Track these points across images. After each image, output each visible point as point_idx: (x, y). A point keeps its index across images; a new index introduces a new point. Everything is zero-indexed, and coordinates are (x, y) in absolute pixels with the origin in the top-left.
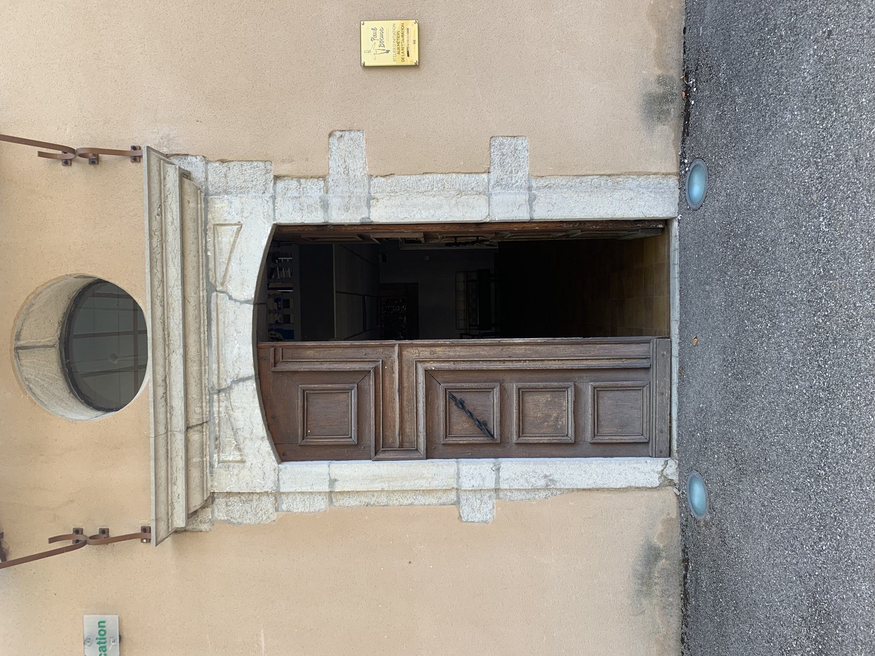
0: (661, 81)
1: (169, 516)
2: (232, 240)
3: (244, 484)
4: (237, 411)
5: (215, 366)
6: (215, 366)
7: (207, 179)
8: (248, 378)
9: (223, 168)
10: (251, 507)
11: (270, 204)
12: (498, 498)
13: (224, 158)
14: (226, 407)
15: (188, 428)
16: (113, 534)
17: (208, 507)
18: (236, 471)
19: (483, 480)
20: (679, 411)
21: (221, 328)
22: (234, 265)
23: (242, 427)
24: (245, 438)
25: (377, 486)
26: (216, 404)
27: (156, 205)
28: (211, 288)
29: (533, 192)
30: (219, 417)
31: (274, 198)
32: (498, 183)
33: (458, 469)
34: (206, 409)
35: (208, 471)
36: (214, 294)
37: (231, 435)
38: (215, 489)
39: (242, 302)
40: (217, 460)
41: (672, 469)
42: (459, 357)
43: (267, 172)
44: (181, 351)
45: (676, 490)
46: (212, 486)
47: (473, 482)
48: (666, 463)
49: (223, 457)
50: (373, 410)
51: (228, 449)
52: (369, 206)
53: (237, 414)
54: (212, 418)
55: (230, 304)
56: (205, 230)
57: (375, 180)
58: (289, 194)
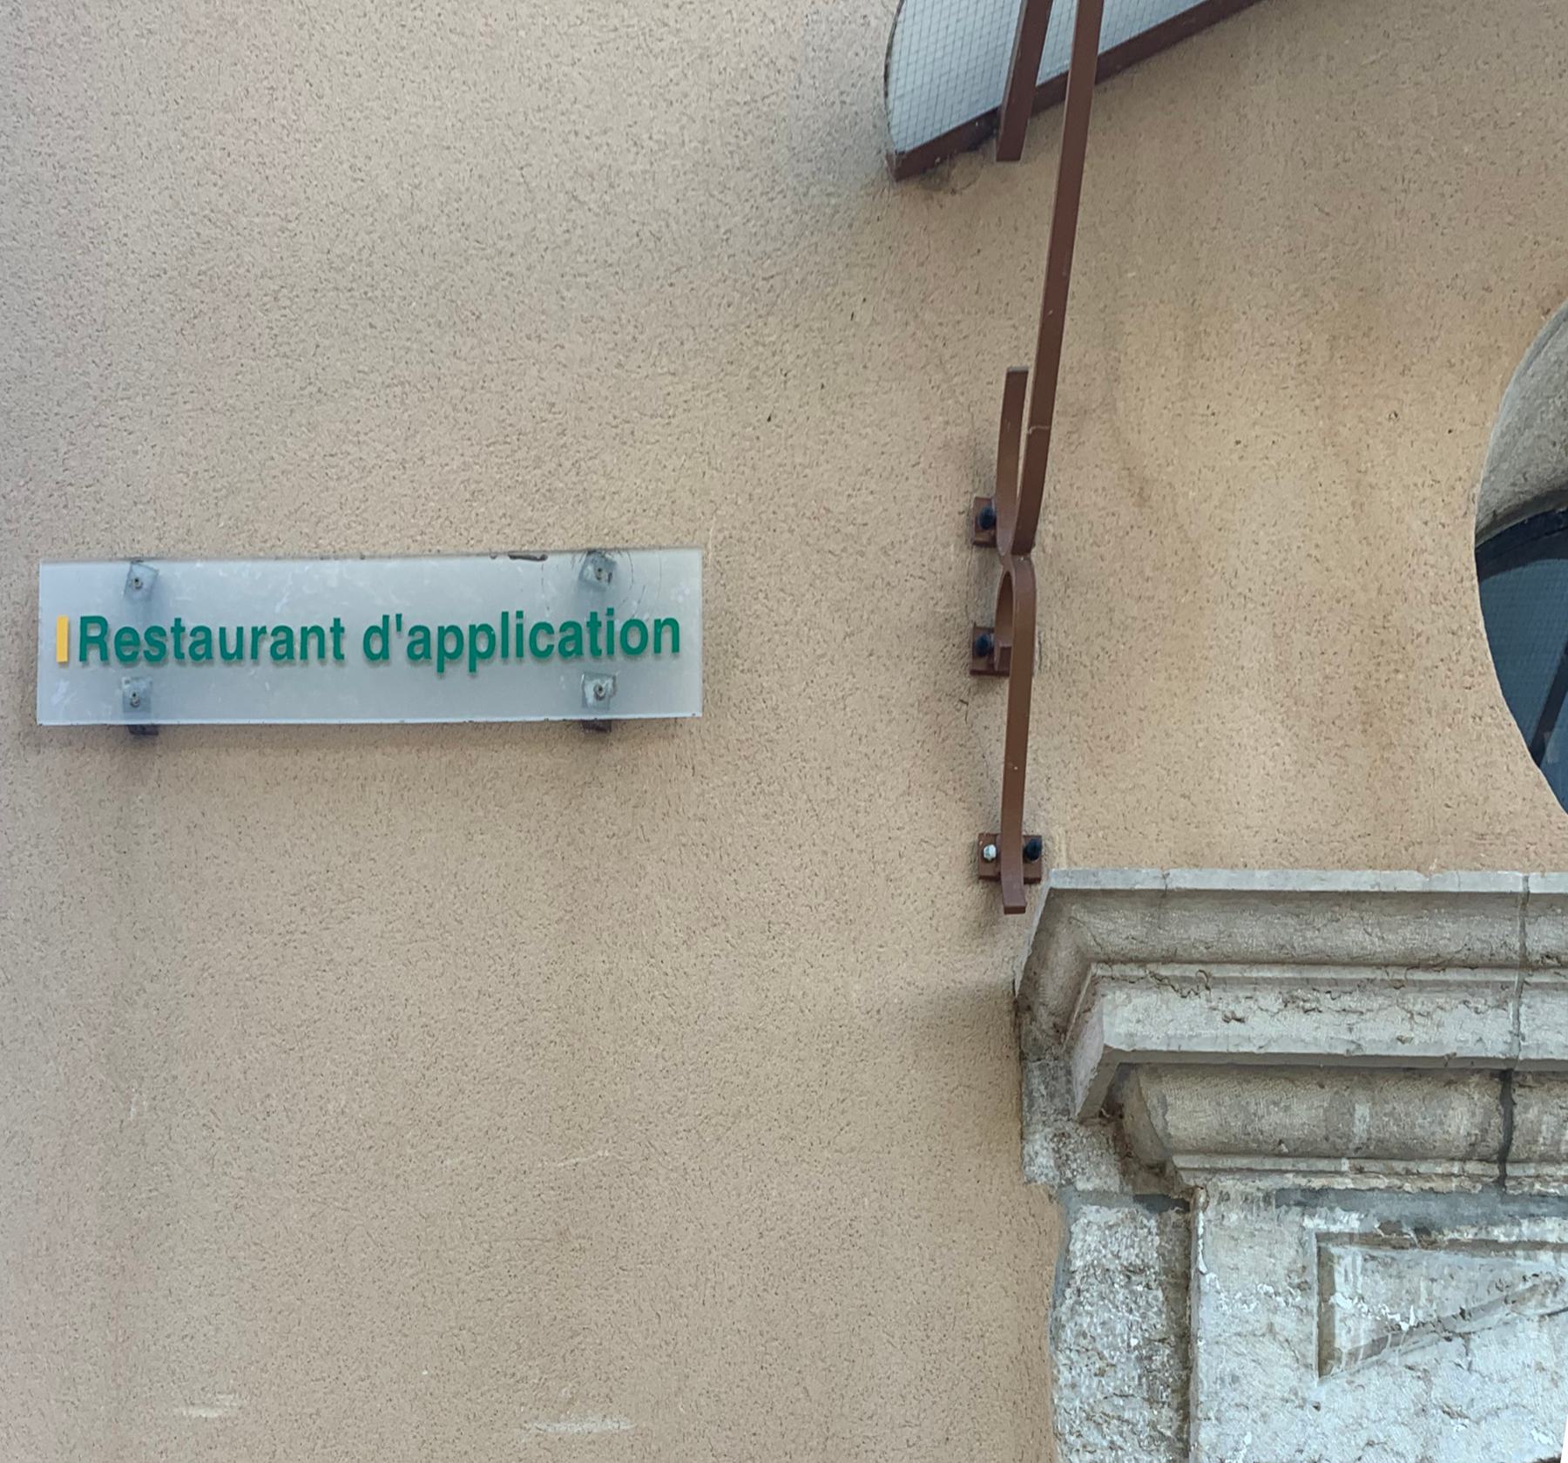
3: (1232, 1365)
4: (1545, 1338)
10: (1124, 1396)
17: (1124, 1173)
18: (1287, 1323)
23: (1478, 1364)
24: (1426, 1376)
30: (1513, 1246)
35: (1290, 1180)
37: (1441, 1305)
38: (1210, 1213)
40: (1334, 1229)
46: (1225, 1197)
49: (1348, 1260)
51: (1383, 1286)
54: (1514, 1208)
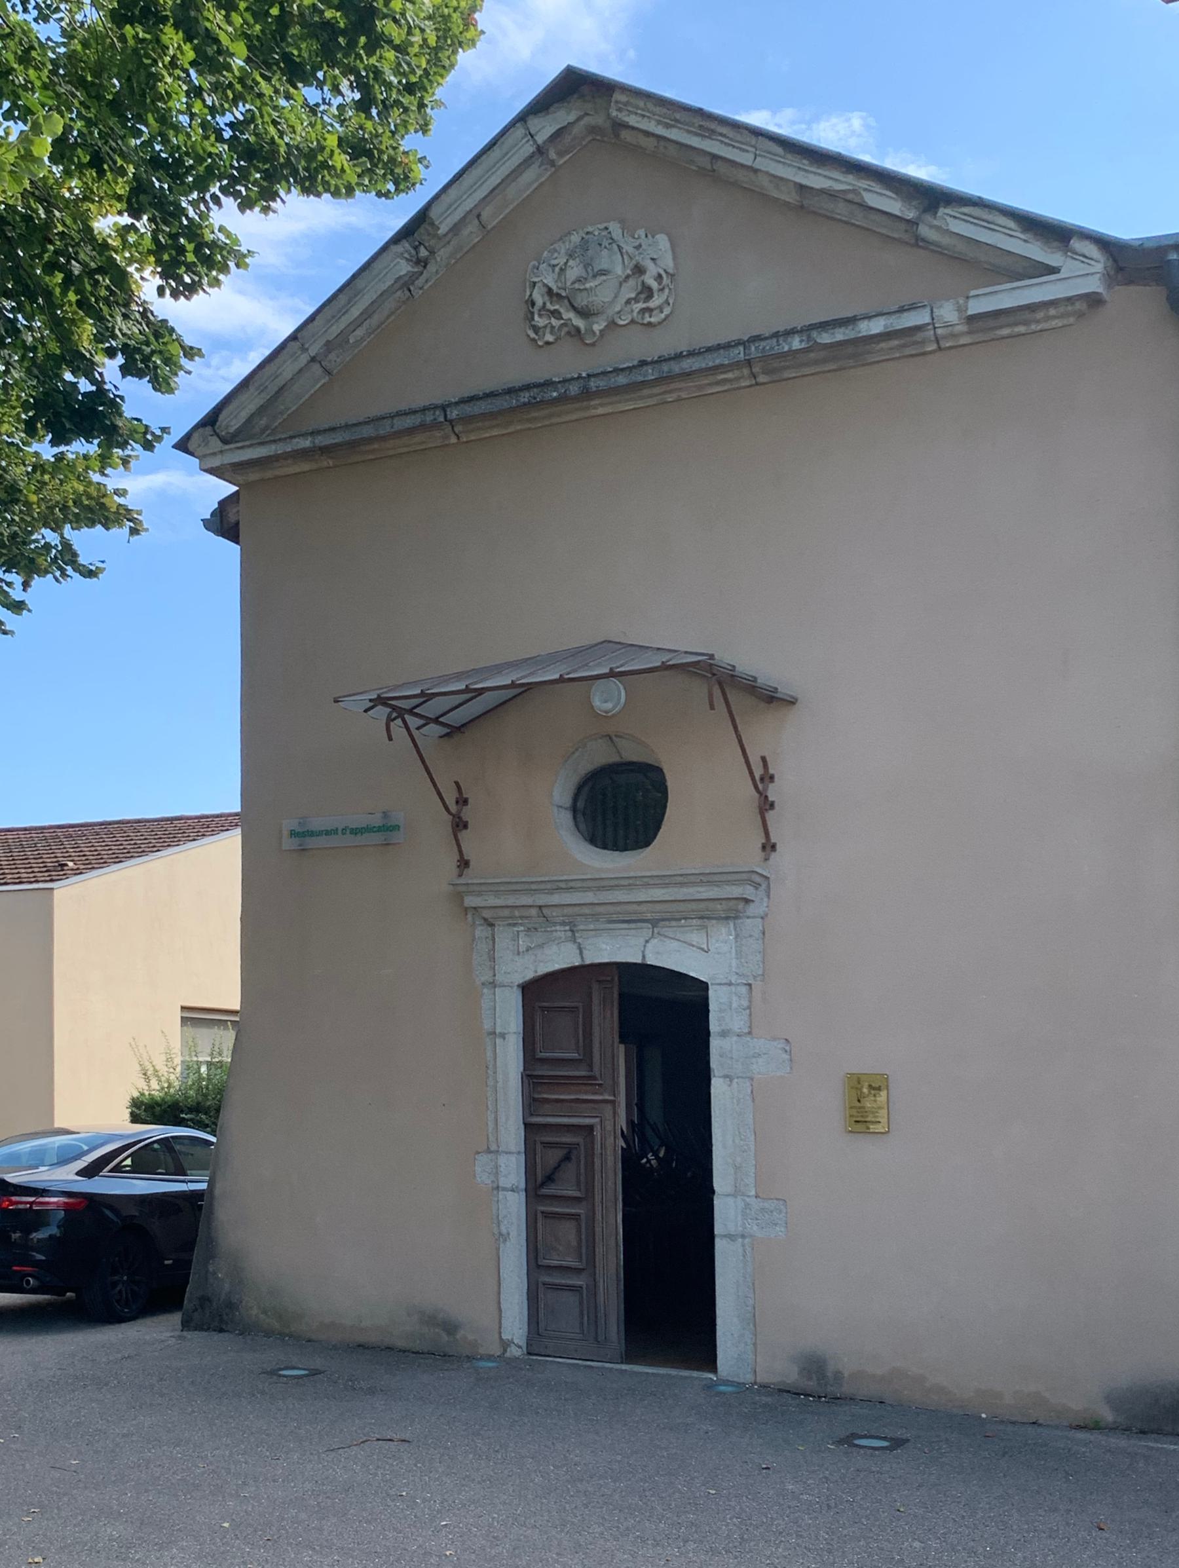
0: (838, 1375)
1: (471, 893)
2: (694, 943)
5: (592, 927)
6: (592, 927)
7: (748, 917)
8: (582, 958)
9: (757, 933)
11: (725, 981)
12: (493, 1189)
13: (766, 935)
14: (560, 938)
15: (540, 907)
16: (464, 835)
19: (506, 1176)
20: (559, 1362)
21: (623, 932)
22: (675, 944)
25: (500, 1077)
26: (562, 928)
27: (710, 878)
28: (654, 923)
29: (740, 1240)
31: (730, 984)
32: (747, 1205)
33: (513, 1153)
34: (558, 920)
36: (650, 926)
39: (643, 952)
41: (514, 1352)
42: (606, 1159)
43: (755, 977)
44: (596, 902)
45: (499, 1354)
47: (503, 1165)
48: (520, 1347)
49: (521, 935)
50: (566, 1074)
52: (726, 1076)
53: (555, 948)
55: (642, 940)
56: (702, 918)
57: (748, 1084)
58: (734, 998)
